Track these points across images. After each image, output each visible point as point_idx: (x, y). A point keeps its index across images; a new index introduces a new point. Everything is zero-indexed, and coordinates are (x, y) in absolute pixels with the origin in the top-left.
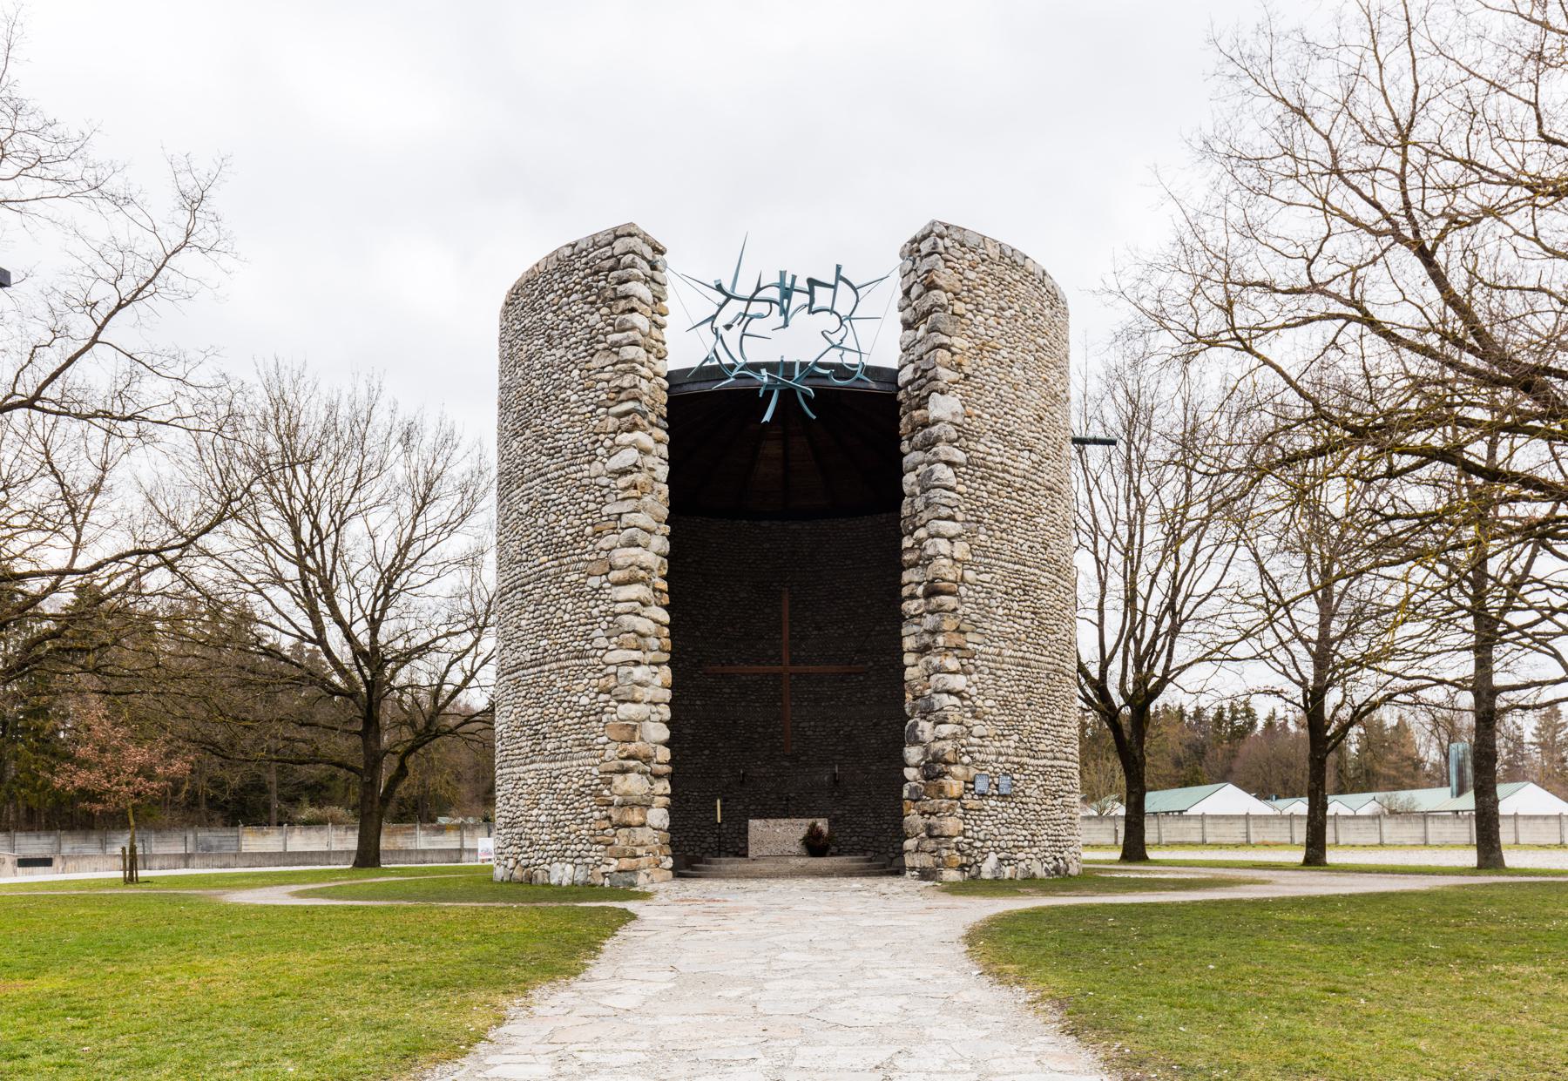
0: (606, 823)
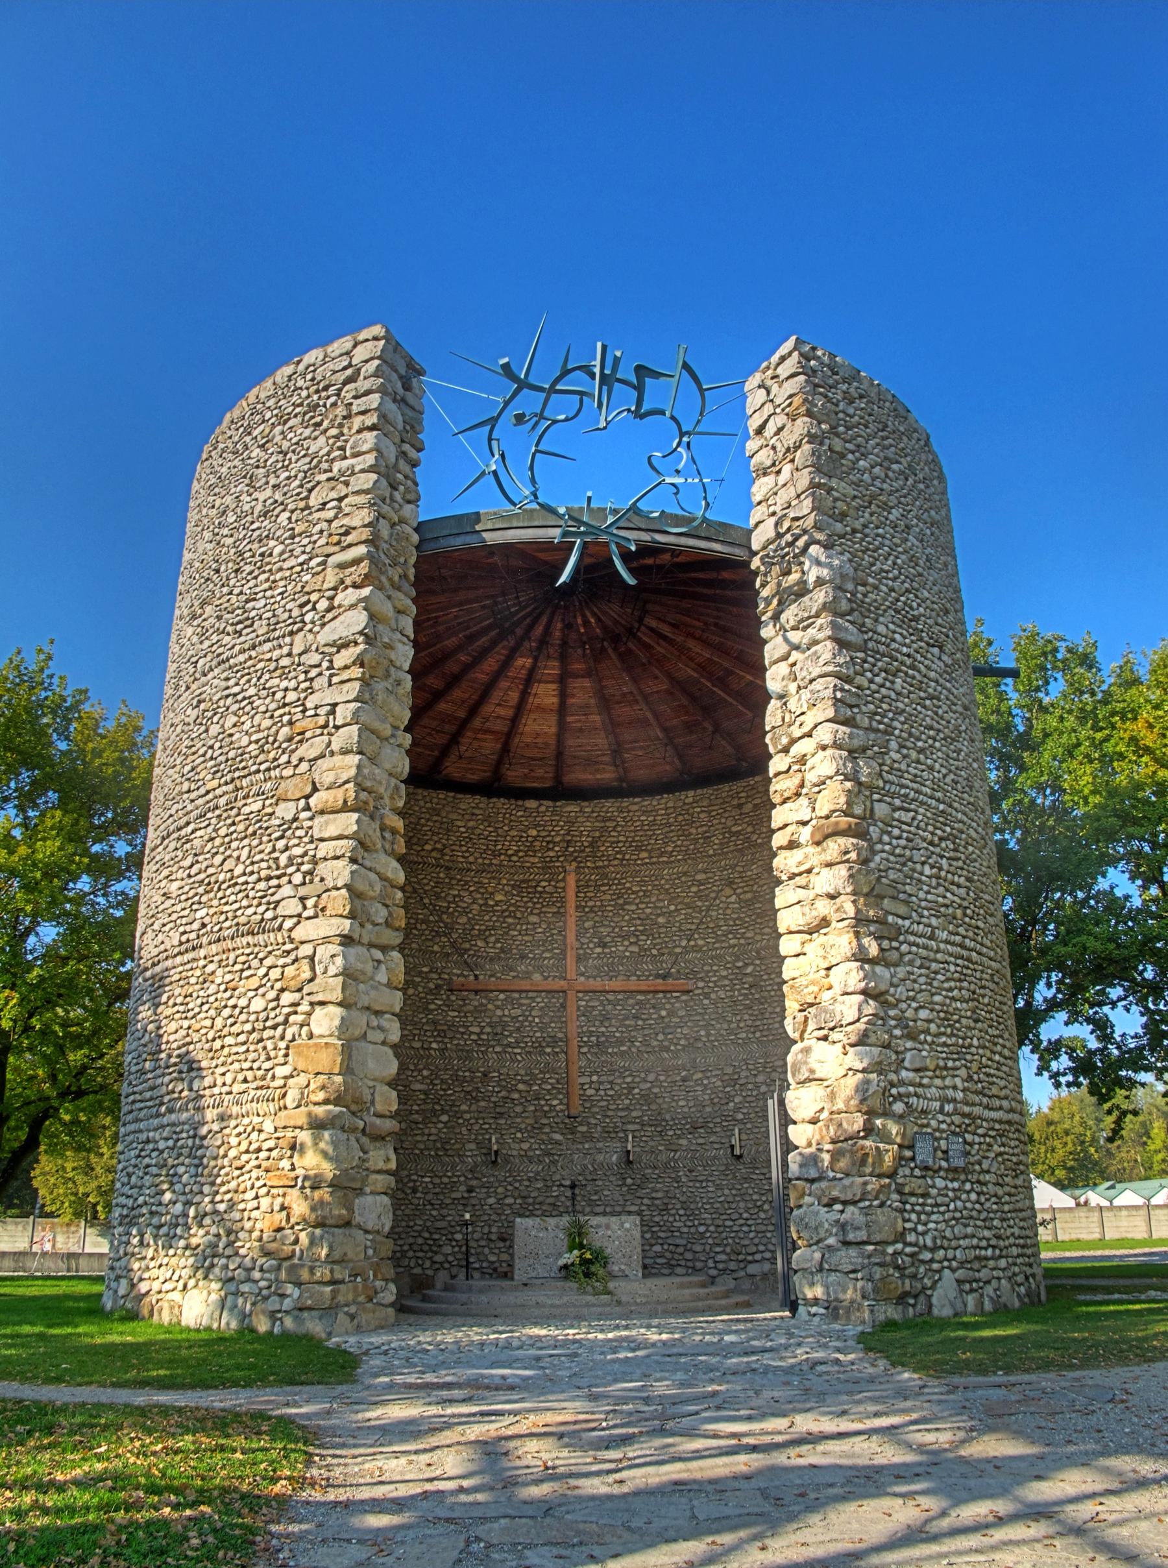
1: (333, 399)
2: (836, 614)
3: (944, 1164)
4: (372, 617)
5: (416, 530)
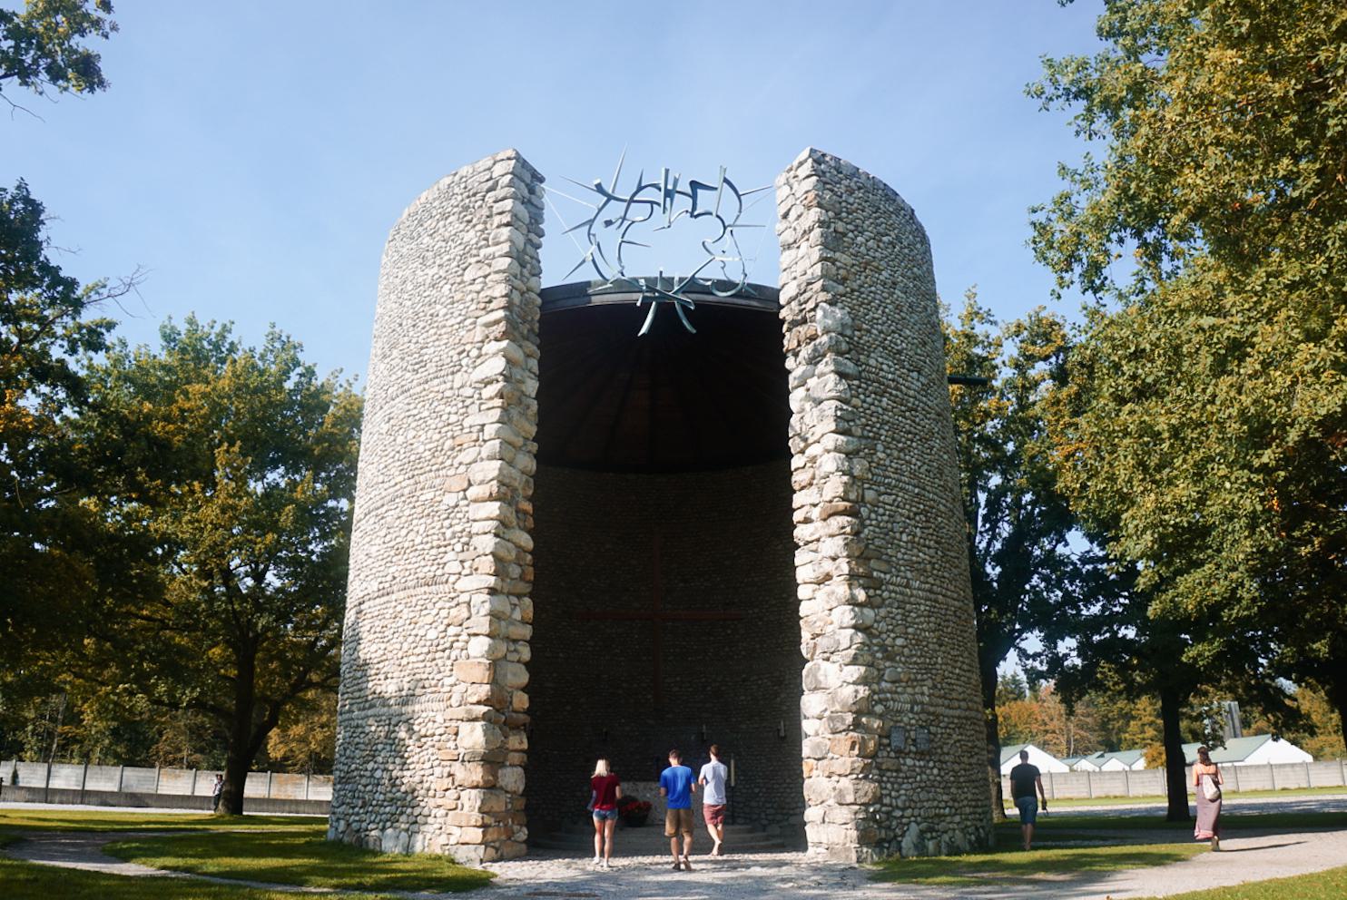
0: (447, 782)
1: (480, 203)
2: (839, 353)
3: (913, 748)
4: (509, 361)
5: (539, 295)
